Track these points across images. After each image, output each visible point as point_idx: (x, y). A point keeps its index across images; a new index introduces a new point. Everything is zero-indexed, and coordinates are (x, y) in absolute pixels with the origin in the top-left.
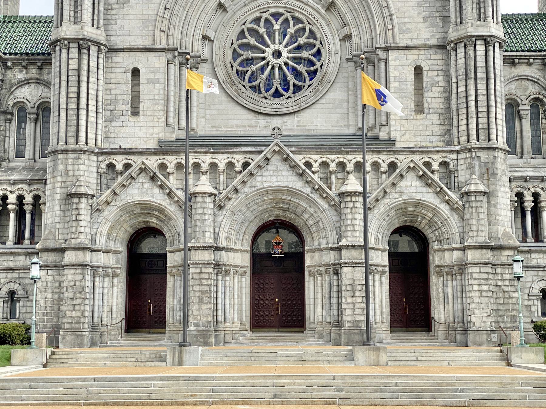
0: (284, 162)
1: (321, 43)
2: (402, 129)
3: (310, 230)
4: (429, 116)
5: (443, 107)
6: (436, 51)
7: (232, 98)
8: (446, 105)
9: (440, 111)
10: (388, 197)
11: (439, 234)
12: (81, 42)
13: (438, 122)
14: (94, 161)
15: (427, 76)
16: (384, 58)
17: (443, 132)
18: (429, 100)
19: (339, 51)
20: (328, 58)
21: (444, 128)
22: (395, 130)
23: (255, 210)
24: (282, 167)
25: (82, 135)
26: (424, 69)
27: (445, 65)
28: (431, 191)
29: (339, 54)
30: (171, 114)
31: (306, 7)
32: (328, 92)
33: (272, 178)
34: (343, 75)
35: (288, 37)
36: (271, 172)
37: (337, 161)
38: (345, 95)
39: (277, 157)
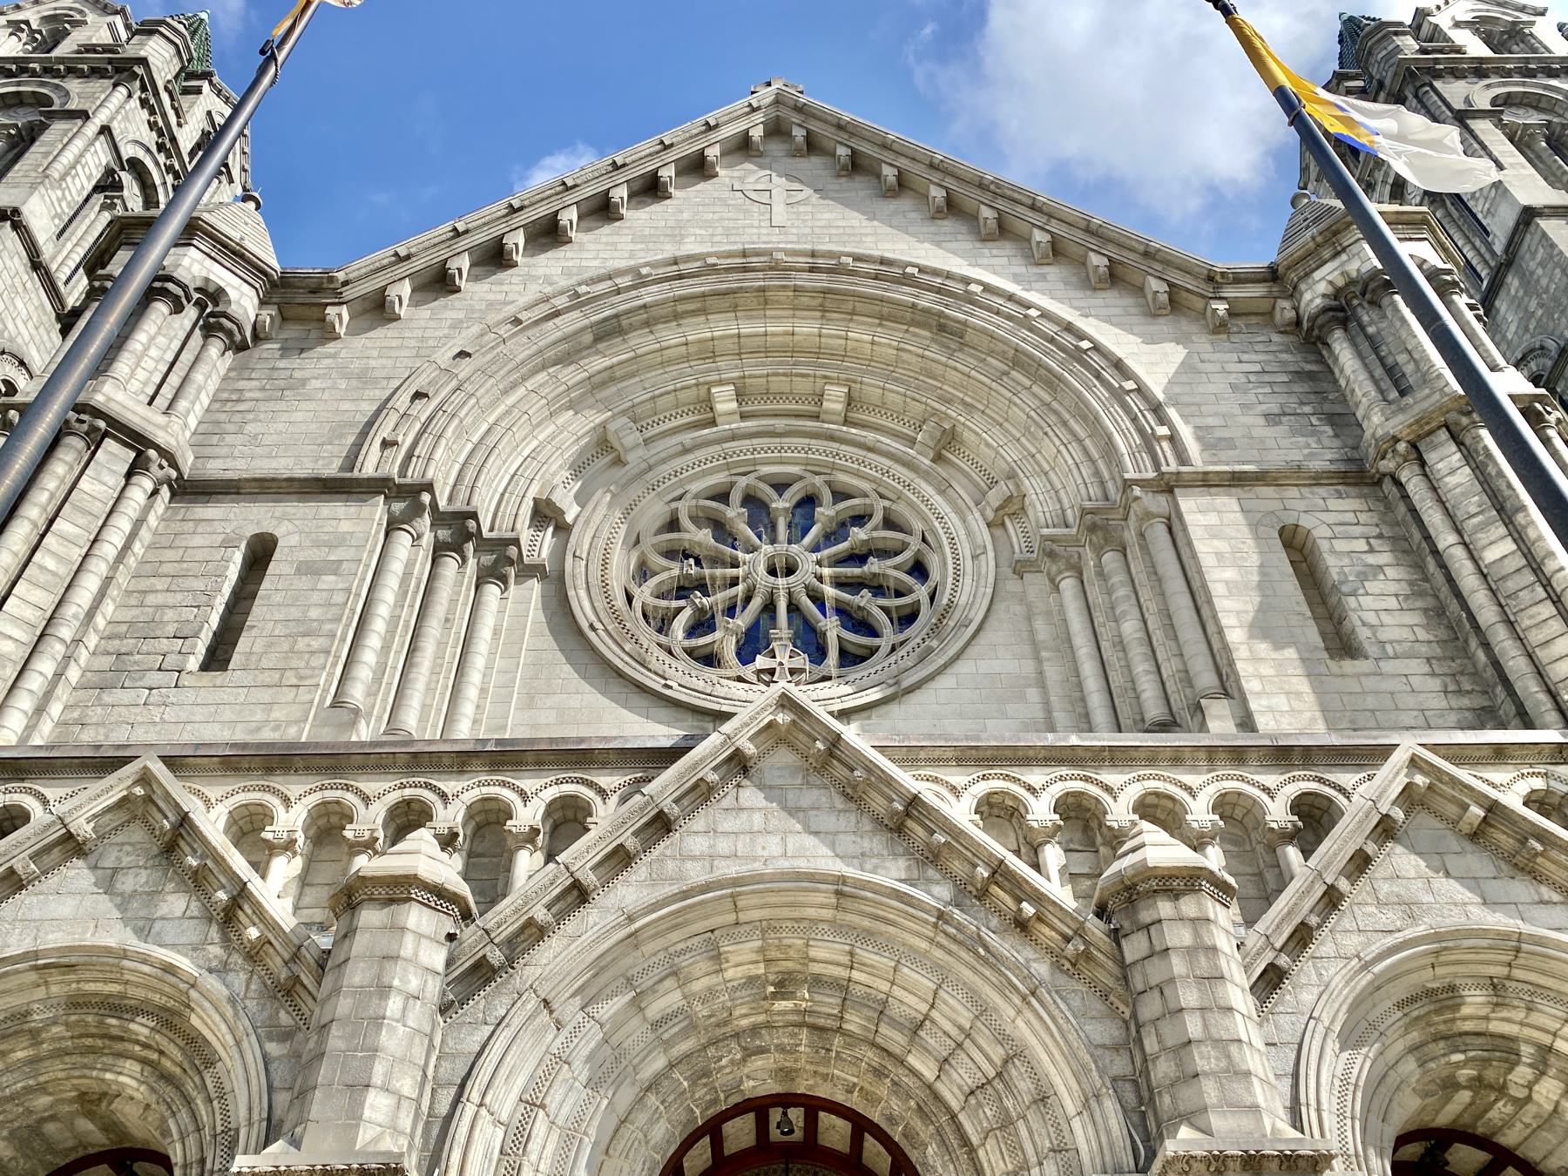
1: (924, 540)
2: (1297, 705)
3: (959, 1128)
4: (1387, 666)
7: (620, 674)
8: (1443, 633)
10: (1347, 923)
15: (1333, 552)
17: (1467, 714)
18: (1371, 618)
19: (990, 547)
20: (951, 570)
21: (1466, 702)
23: (675, 1014)
24: (809, 797)
26: (1315, 533)
27: (1385, 522)
28: (1556, 897)
29: (991, 554)
30: (364, 672)
31: (870, 455)
32: (964, 656)
33: (760, 839)
34: (1008, 611)
36: (758, 818)
38: (1029, 667)
39: (784, 757)
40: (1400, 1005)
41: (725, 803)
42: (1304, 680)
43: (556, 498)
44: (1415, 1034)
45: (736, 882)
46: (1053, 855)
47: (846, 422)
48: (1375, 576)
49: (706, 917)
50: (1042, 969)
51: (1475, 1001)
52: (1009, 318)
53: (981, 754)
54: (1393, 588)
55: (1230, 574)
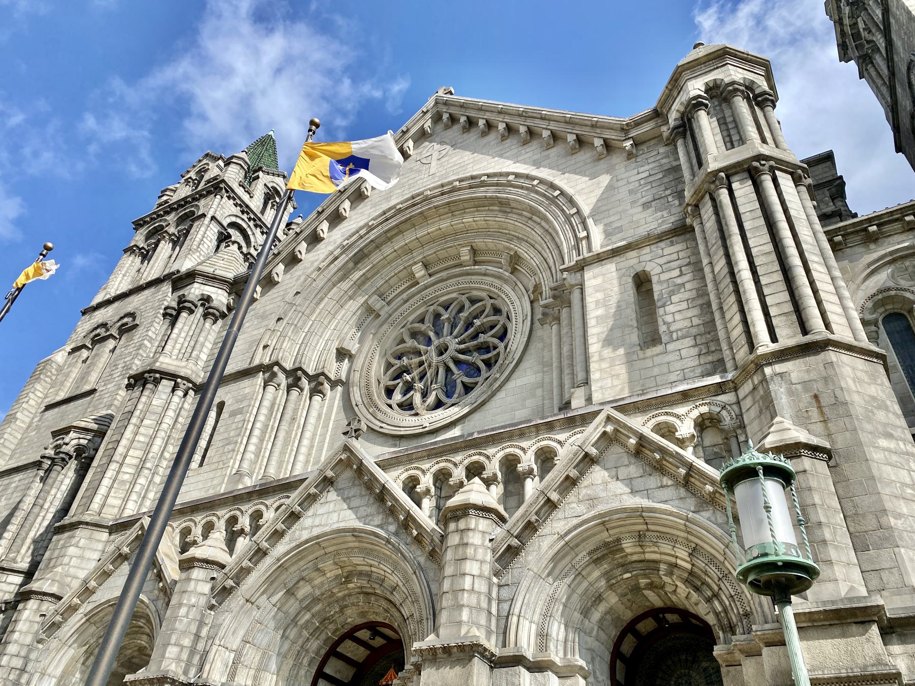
0: (357, 482)
4: (670, 347)
5: (701, 322)
6: (672, 242)
9: (694, 331)
11: (725, 610)
12: (146, 375)
13: (695, 351)
14: (99, 541)
15: (660, 282)
16: (577, 282)
17: (708, 366)
18: (669, 319)
21: (710, 358)
22: (602, 388)
25: (98, 499)
26: (652, 273)
28: (670, 482)
35: (471, 330)
37: (466, 462)
39: (348, 474)
40: (589, 554)
41: (322, 501)
42: (623, 366)
43: (345, 346)
44: (605, 566)
45: (318, 537)
46: (427, 503)
47: (476, 263)
48: (680, 289)
49: (314, 552)
50: (422, 560)
51: (628, 546)
52: (522, 188)
53: (438, 451)
54: (687, 295)
55: (600, 312)
